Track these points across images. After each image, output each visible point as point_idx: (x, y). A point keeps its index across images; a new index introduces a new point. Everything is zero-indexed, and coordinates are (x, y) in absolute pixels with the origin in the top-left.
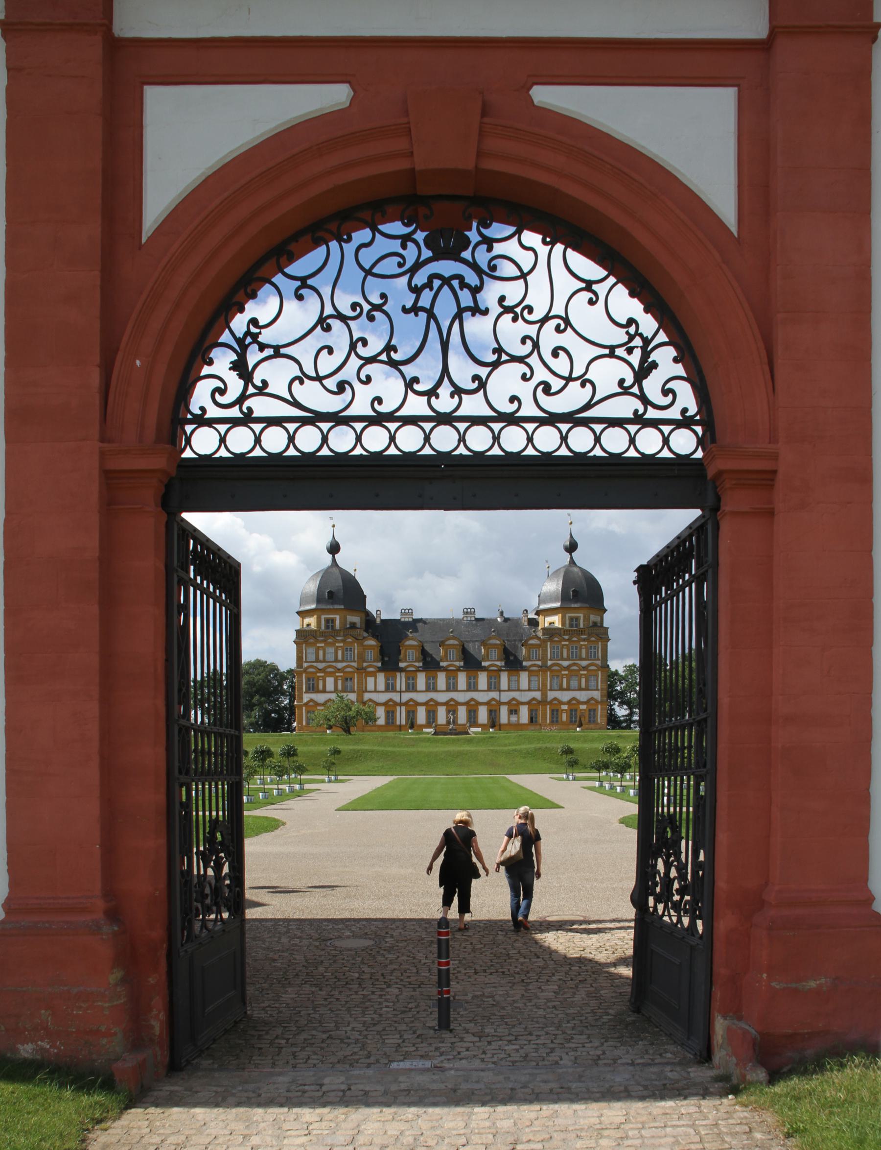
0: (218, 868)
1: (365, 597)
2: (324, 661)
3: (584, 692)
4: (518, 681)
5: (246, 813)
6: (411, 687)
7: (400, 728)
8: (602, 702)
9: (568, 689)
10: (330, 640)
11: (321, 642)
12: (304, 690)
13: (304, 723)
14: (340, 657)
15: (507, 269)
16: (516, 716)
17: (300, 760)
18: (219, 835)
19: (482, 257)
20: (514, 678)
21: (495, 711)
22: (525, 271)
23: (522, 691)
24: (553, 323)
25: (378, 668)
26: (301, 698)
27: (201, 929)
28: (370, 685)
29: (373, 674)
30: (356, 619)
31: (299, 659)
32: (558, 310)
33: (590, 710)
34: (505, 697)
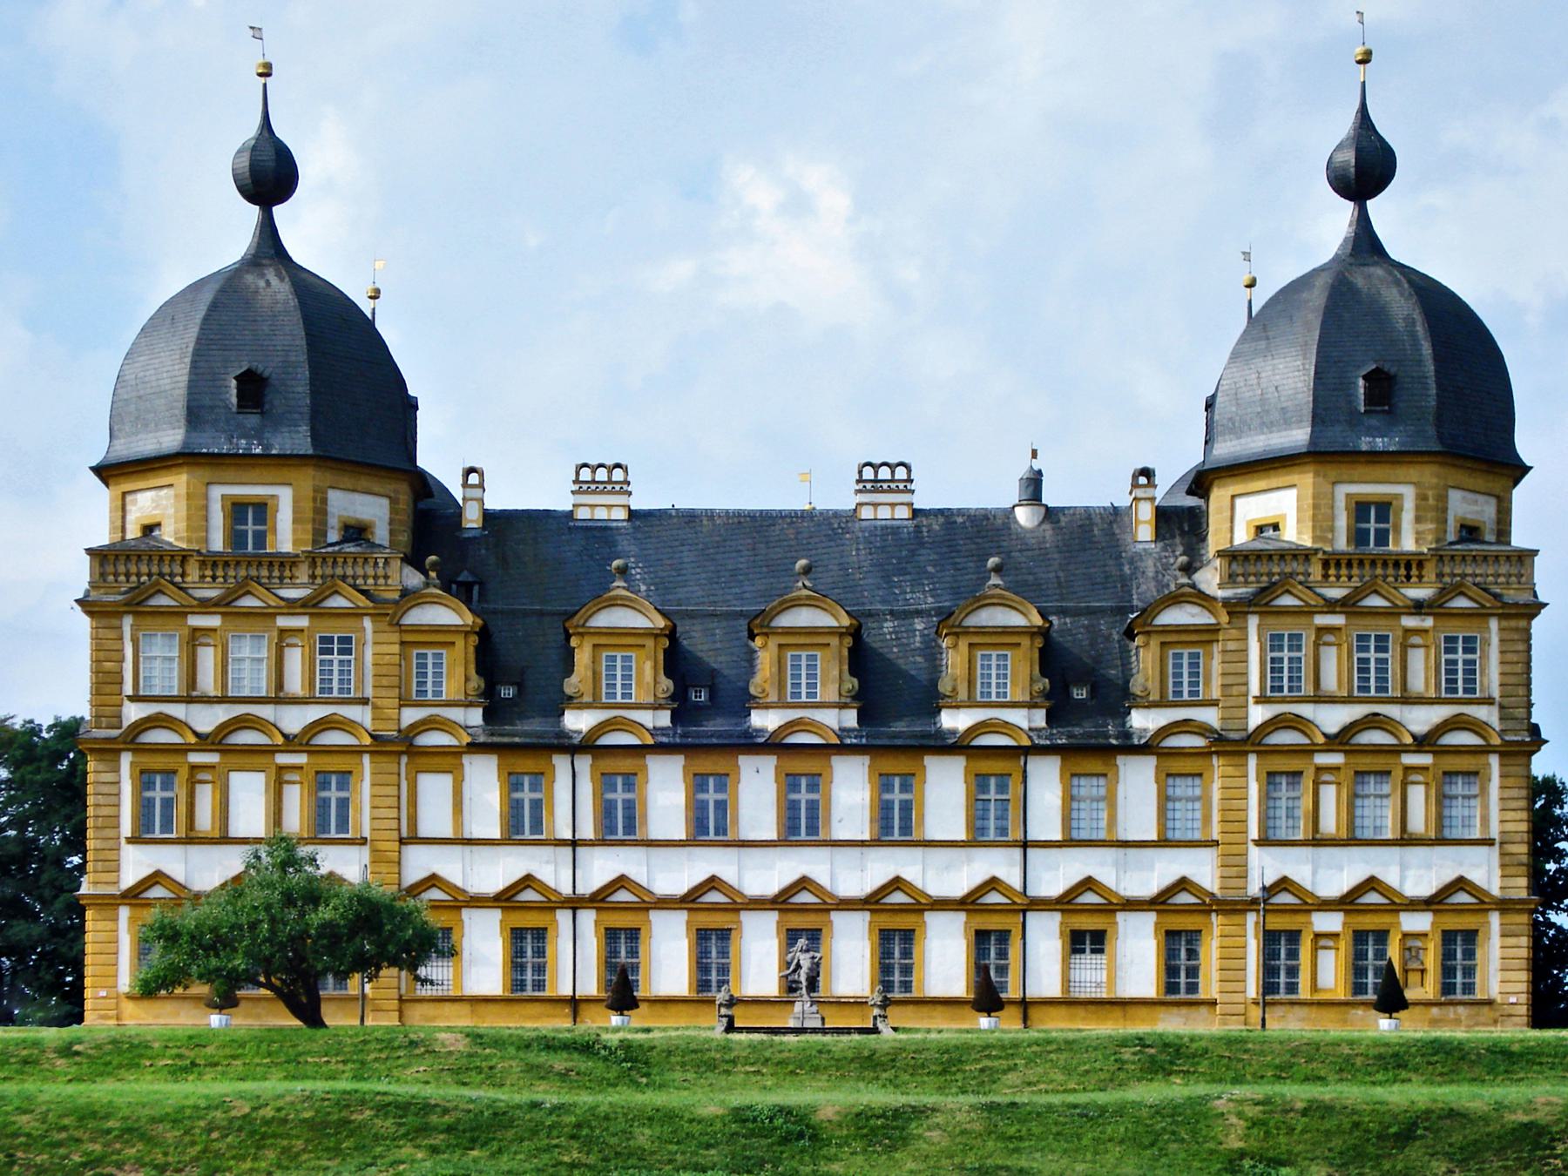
1: (412, 405)
2: (223, 700)
4: (1111, 800)
11: (206, 606)
14: (295, 683)
23: (1126, 844)
28: (435, 817)
31: (105, 682)
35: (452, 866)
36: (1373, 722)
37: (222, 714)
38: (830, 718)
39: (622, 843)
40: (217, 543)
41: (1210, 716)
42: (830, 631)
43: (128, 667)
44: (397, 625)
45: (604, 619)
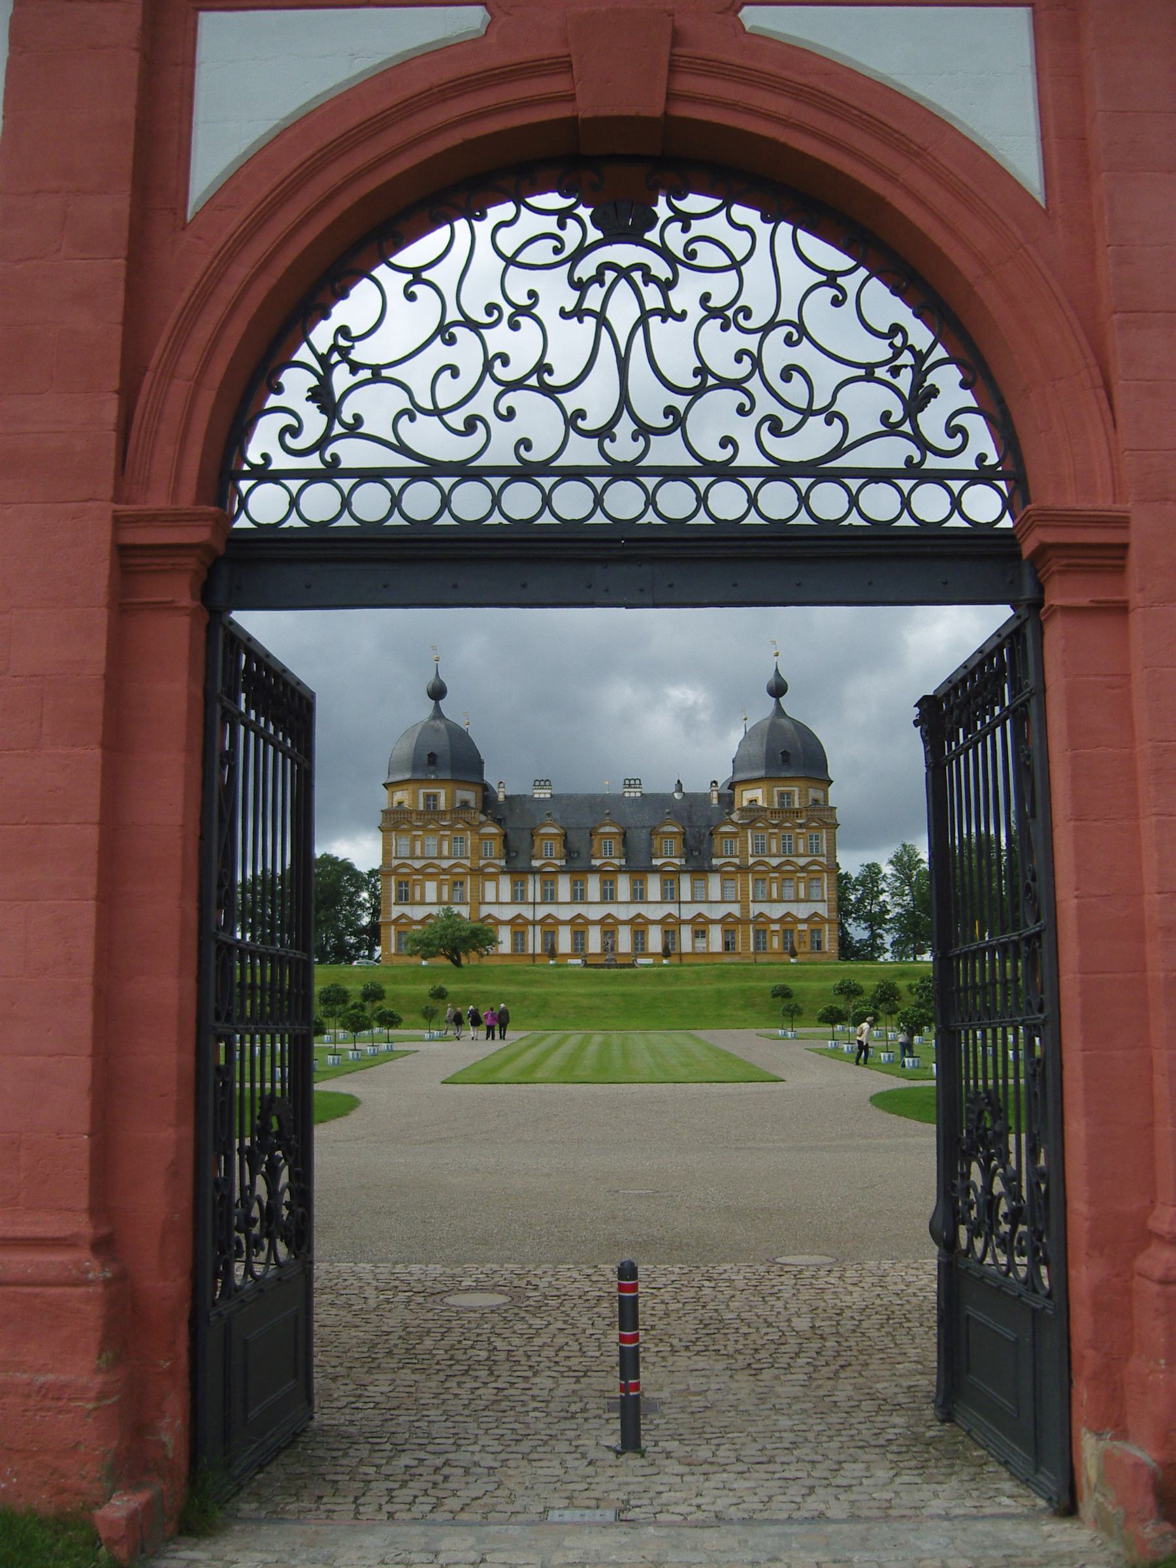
0: (272, 1177)
3: (802, 905)
4: (706, 888)
5: (317, 1087)
6: (549, 897)
7: (534, 956)
8: (829, 921)
9: (780, 900)
10: (431, 826)
11: (418, 828)
12: (393, 900)
13: (393, 950)
14: (446, 852)
15: (708, 255)
16: (704, 940)
17: (387, 1006)
18: (274, 1120)
19: (675, 239)
20: (702, 884)
21: (673, 932)
22: (739, 258)
23: (711, 902)
24: (783, 331)
25: (501, 867)
26: (389, 913)
27: (245, 1276)
28: (490, 896)
29: (493, 877)
30: (469, 795)
31: (386, 853)
32: (788, 312)
33: (813, 931)
34: (688, 912)
35: (496, 911)
36: (788, 863)
37: (422, 863)
38: (616, 862)
39: (549, 903)
40: (421, 807)
41: (737, 861)
42: (616, 833)
43: (394, 847)
44: (478, 833)
45: (543, 831)
